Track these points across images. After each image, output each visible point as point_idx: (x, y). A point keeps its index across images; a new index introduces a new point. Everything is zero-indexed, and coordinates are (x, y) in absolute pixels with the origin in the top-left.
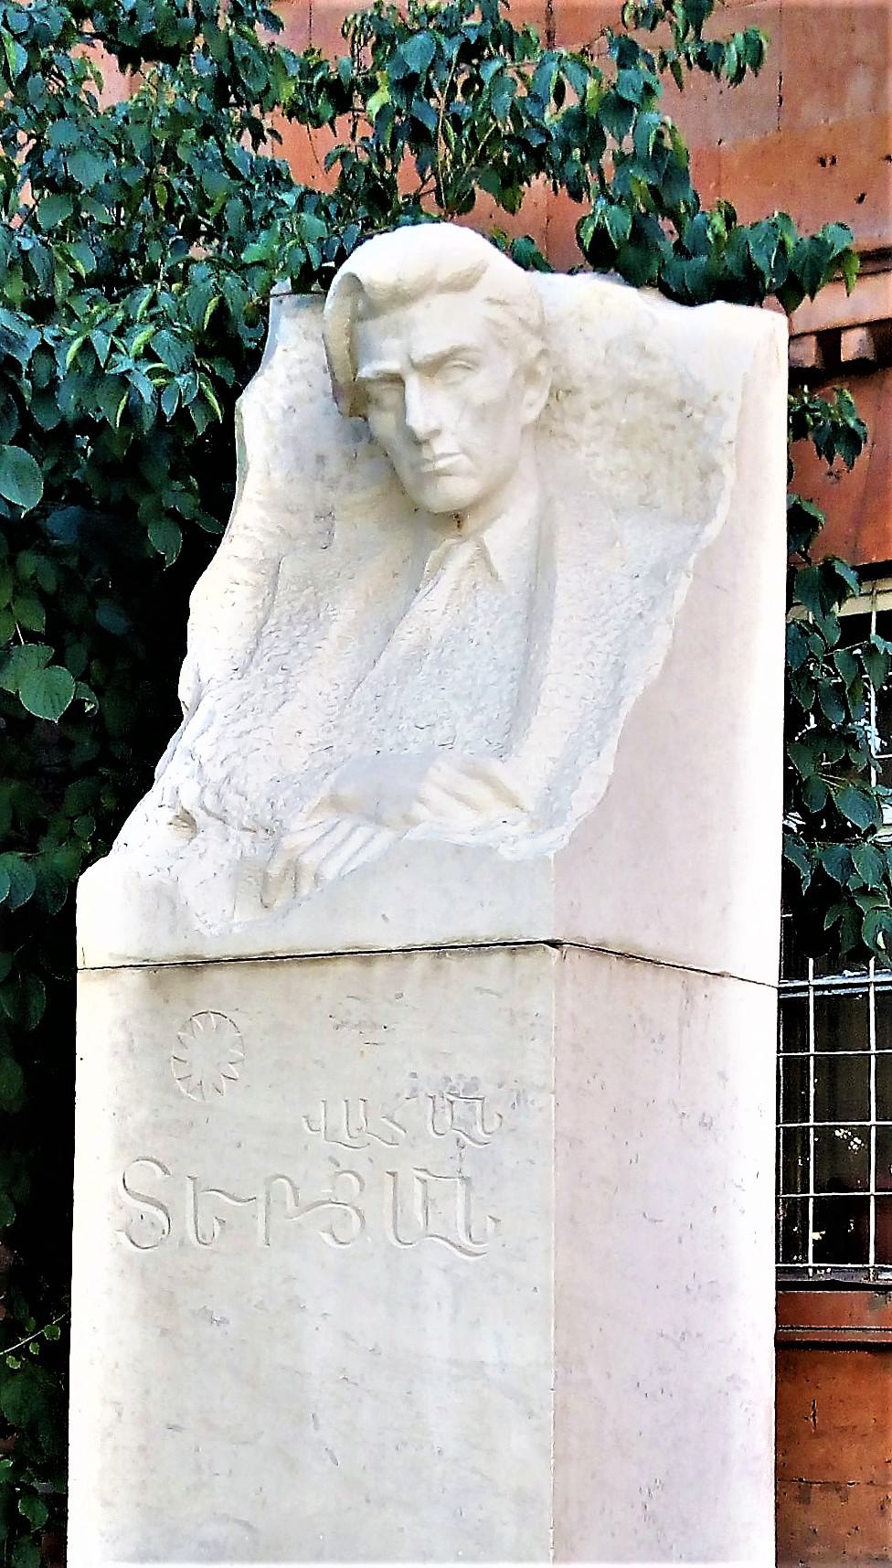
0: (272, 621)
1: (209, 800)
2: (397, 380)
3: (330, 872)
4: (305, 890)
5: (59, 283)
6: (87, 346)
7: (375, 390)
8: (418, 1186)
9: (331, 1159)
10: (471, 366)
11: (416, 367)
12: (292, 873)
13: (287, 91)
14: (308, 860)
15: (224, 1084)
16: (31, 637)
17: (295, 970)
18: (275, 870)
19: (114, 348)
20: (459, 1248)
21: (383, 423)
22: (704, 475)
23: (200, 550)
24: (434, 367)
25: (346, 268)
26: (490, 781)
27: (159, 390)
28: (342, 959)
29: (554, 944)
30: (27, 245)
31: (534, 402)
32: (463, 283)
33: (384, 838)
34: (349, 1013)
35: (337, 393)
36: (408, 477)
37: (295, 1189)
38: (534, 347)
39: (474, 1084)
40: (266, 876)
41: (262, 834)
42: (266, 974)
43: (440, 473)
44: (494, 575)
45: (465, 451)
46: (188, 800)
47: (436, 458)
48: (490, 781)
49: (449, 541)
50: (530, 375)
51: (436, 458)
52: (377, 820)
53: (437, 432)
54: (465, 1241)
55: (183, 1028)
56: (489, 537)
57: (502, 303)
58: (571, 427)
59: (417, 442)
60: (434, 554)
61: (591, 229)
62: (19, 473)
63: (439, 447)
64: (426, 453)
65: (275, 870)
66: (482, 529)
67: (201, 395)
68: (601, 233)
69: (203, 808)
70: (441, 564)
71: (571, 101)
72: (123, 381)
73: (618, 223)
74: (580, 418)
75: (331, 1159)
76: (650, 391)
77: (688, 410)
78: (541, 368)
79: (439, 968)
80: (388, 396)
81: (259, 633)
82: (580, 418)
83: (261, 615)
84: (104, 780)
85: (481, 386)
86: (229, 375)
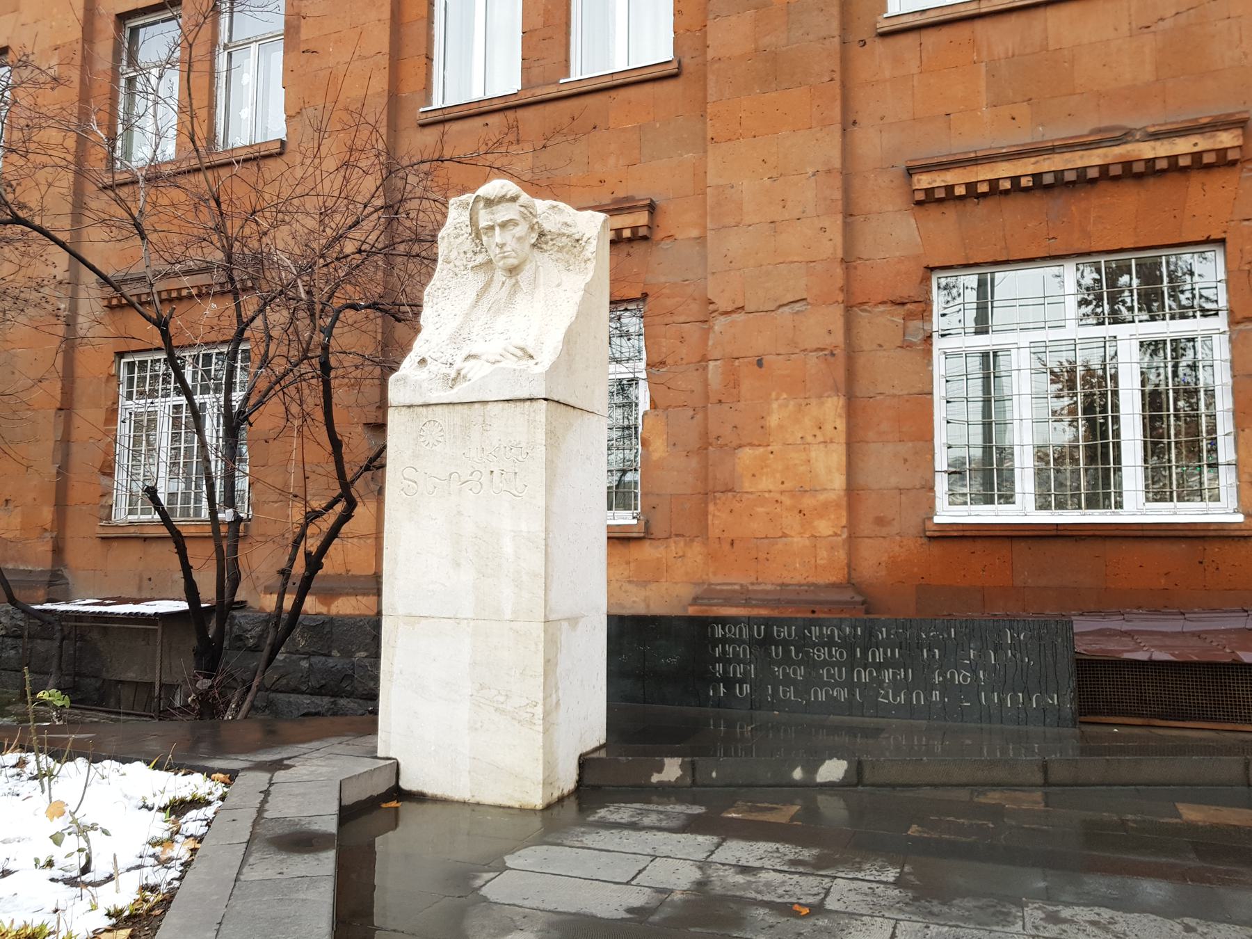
31: (535, 236)
32: (514, 199)
37: (459, 476)
58: (544, 246)
74: (546, 243)
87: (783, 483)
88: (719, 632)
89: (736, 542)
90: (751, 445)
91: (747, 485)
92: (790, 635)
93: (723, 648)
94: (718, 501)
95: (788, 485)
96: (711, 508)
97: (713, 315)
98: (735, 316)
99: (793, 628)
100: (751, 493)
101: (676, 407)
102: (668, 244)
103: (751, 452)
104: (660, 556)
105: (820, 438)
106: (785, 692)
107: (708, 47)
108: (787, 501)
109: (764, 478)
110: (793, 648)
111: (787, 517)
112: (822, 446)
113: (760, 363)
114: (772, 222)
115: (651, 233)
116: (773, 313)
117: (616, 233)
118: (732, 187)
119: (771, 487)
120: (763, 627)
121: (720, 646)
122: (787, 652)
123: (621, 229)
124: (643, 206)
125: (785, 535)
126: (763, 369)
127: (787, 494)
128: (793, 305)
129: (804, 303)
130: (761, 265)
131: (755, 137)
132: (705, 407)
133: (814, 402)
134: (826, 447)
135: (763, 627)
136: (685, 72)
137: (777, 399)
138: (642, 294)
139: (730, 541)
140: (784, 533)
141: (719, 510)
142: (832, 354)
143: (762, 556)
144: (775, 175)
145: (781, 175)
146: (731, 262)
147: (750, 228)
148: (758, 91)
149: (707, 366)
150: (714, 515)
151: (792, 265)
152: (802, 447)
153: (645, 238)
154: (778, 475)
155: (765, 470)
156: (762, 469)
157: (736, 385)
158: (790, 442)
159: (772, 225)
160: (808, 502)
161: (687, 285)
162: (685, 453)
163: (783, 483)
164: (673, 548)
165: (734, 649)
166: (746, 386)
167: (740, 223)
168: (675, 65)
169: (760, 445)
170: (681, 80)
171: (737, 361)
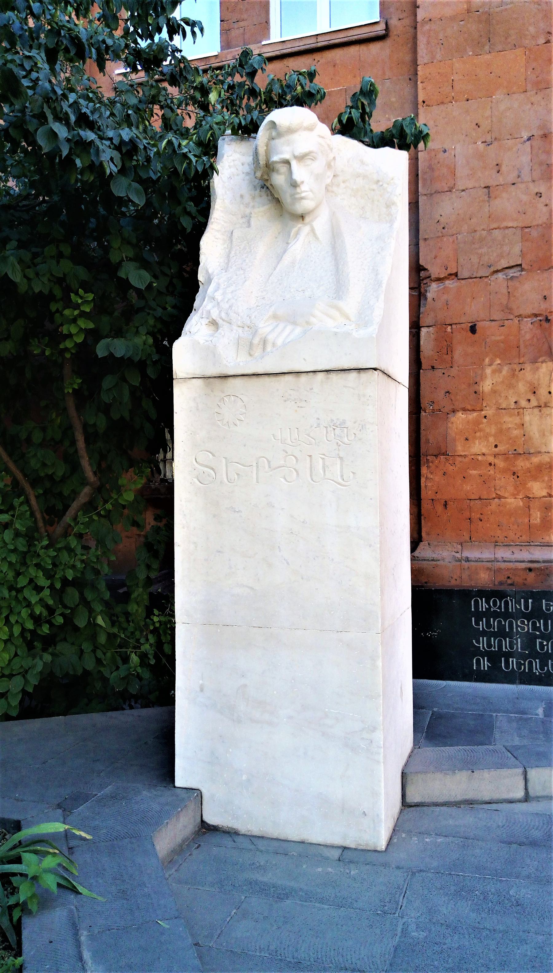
0: (233, 252)
1: (223, 315)
2: (287, 162)
3: (279, 342)
4: (269, 348)
8: (321, 461)
9: (284, 450)
10: (314, 159)
11: (295, 157)
12: (262, 343)
14: (271, 338)
15: (238, 422)
17: (267, 379)
20: (339, 484)
22: (388, 206)
24: (301, 158)
26: (338, 309)
28: (286, 376)
33: (298, 330)
34: (290, 395)
37: (269, 462)
39: (344, 422)
41: (246, 328)
43: (302, 198)
44: (317, 238)
45: (311, 191)
46: (215, 315)
47: (302, 192)
48: (338, 309)
49: (300, 225)
51: (302, 192)
52: (295, 323)
53: (303, 182)
54: (340, 481)
55: (220, 401)
56: (315, 224)
57: (323, 137)
60: (294, 230)
62: (137, 192)
63: (303, 188)
64: (298, 190)
65: (256, 341)
66: (312, 221)
69: (221, 318)
70: (297, 233)
74: (338, 186)
76: (365, 177)
77: (381, 183)
79: (328, 378)
80: (283, 169)
82: (338, 186)
83: (227, 250)
87: (496, 446)
88: (483, 605)
89: (450, 503)
90: (464, 410)
91: (460, 449)
93: (488, 622)
94: (431, 464)
95: (502, 448)
97: (425, 281)
100: (465, 456)
105: (534, 403)
107: (418, 7)
108: (500, 463)
109: (477, 442)
111: (500, 479)
112: (536, 411)
113: (473, 329)
114: (485, 187)
116: (486, 280)
118: (445, 151)
119: (484, 450)
128: (507, 271)
129: (519, 269)
130: (475, 231)
133: (528, 367)
134: (540, 411)
136: (394, 32)
137: (490, 365)
139: (443, 502)
140: (497, 494)
141: (432, 473)
142: (547, 320)
144: (489, 139)
145: (496, 139)
147: (463, 193)
148: (471, 53)
150: (427, 478)
151: (507, 231)
152: (516, 411)
154: (491, 439)
155: (478, 434)
157: (449, 350)
158: (504, 406)
160: (521, 464)
163: (496, 446)
166: (458, 353)
167: (452, 188)
168: (382, 26)
169: (474, 410)
170: (387, 43)
171: (449, 327)
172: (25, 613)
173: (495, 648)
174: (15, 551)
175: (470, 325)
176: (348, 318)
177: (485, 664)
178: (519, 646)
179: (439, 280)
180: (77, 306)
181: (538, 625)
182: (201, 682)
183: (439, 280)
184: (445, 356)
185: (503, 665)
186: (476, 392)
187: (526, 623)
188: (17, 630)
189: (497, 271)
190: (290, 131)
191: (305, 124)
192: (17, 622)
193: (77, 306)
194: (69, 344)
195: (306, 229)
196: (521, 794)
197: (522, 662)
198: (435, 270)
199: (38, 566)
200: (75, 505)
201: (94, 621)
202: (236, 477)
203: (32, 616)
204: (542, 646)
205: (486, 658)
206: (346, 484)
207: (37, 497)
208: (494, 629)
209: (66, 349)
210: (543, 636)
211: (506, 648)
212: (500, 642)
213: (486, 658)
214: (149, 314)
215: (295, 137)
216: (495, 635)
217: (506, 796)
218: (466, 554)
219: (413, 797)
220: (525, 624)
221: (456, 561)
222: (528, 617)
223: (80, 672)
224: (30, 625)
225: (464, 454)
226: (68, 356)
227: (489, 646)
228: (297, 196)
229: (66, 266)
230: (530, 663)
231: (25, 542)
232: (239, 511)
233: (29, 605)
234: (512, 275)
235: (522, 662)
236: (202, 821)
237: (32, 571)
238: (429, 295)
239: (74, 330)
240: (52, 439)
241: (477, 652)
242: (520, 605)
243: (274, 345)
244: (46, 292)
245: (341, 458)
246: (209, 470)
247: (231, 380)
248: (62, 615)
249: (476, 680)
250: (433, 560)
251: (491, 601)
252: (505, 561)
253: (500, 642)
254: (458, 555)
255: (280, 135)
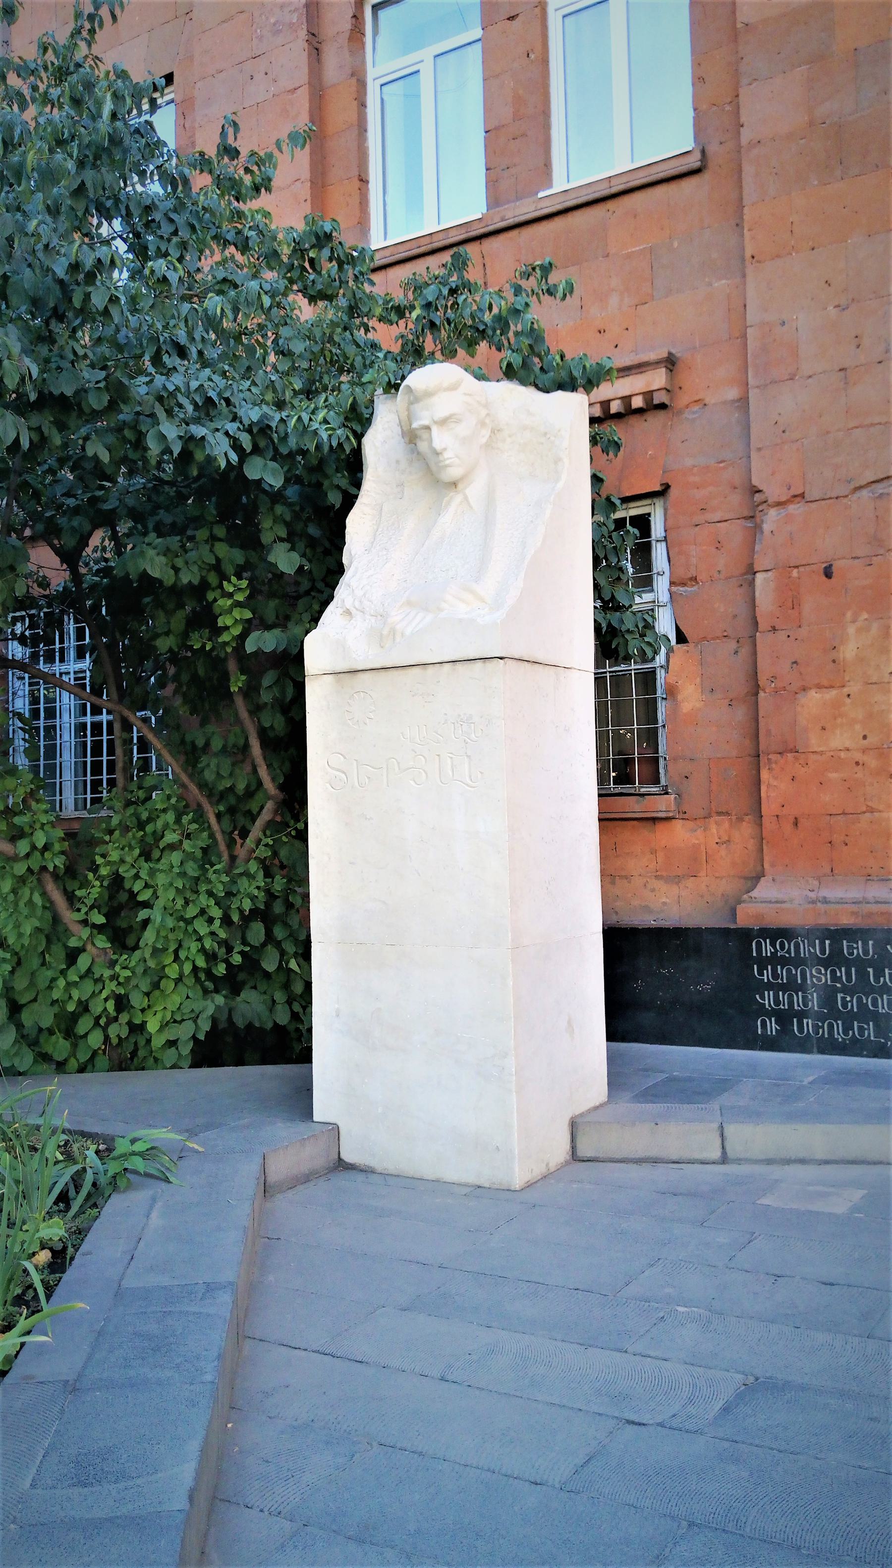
0: (380, 530)
1: (357, 604)
2: (428, 428)
3: (408, 632)
4: (398, 639)
5: (287, 393)
6: (300, 418)
7: (419, 433)
8: (449, 761)
9: (413, 750)
10: (458, 421)
11: (435, 422)
13: (378, 311)
15: (368, 721)
16: (282, 540)
18: (385, 632)
19: (311, 420)
20: (468, 785)
21: (423, 446)
22: (556, 463)
23: (349, 501)
24: (443, 422)
25: (405, 383)
27: (330, 436)
29: (501, 658)
30: (273, 378)
31: (486, 433)
32: (453, 388)
35: (404, 434)
36: (434, 468)
37: (398, 763)
38: (484, 412)
40: (381, 635)
41: (379, 617)
42: (383, 673)
45: (457, 457)
46: (348, 604)
47: (445, 460)
49: (451, 494)
50: (483, 424)
51: (445, 460)
53: (445, 449)
55: (350, 699)
56: (468, 491)
57: (470, 395)
59: (437, 454)
61: (505, 363)
62: (274, 473)
63: (446, 455)
64: (441, 458)
65: (385, 632)
67: (348, 437)
68: (509, 365)
70: (449, 503)
71: (495, 310)
72: (315, 432)
73: (517, 360)
75: (413, 750)
77: (548, 436)
78: (487, 421)
80: (424, 435)
81: (375, 535)
83: (375, 527)
84: (314, 597)
85: (463, 429)
86: (359, 429)
87: (865, 737)
88: (768, 949)
89: (803, 822)
90: (819, 687)
91: (814, 742)
92: (866, 952)
93: (774, 971)
94: (774, 766)
95: (873, 740)
96: (765, 775)
97: (760, 508)
98: (792, 508)
99: (871, 942)
100: (821, 753)
101: (713, 639)
102: (694, 413)
103: (818, 696)
104: (697, 842)
106: (861, 1029)
107: (742, 126)
109: (838, 732)
110: (870, 970)
113: (828, 573)
114: (840, 370)
115: (671, 399)
116: (845, 501)
117: (623, 402)
118: (783, 324)
119: (848, 744)
120: (827, 942)
121: (769, 967)
122: (863, 975)
123: (629, 397)
124: (657, 363)
125: (872, 810)
126: (833, 579)
127: (871, 752)
128: (874, 486)
130: (828, 432)
131: (813, 249)
132: (753, 637)
135: (827, 942)
136: (712, 164)
137: (854, 621)
138: (662, 485)
139: (792, 820)
140: (868, 806)
141: (776, 778)
143: (837, 838)
146: (784, 432)
147: (810, 380)
148: (816, 183)
149: (754, 579)
150: (769, 786)
151: (872, 429)
153: (663, 406)
154: (858, 727)
155: (839, 720)
156: (835, 718)
157: (796, 604)
158: (874, 679)
159: (842, 374)
161: (724, 468)
162: (727, 702)
163: (865, 737)
164: (714, 831)
165: (789, 971)
166: (808, 607)
167: (795, 375)
168: (697, 155)
169: (832, 687)
170: (706, 176)
171: (795, 571)
172: (194, 946)
173: (784, 1005)
174: (183, 874)
175: (825, 565)
176: (482, 600)
177: (773, 1027)
178: (815, 1003)
179: (779, 504)
180: (230, 595)
181: (838, 974)
182: (337, 1006)
183: (779, 504)
184: (790, 611)
185: (795, 1028)
186: (834, 661)
187: (823, 972)
188: (187, 968)
189: (861, 487)
190: (428, 394)
191: (445, 385)
192: (187, 958)
193: (230, 595)
194: (225, 637)
195: (458, 498)
196: (716, 1154)
197: (820, 1024)
198: (773, 491)
199: (210, 894)
200: (260, 823)
201: (287, 965)
202: (367, 780)
203: (203, 950)
204: (845, 1005)
205: (773, 1019)
206: (473, 785)
207: (219, 816)
208: (782, 979)
209: (226, 644)
210: (845, 990)
211: (799, 1006)
212: (790, 997)
213: (773, 1019)
214: (314, 597)
215: (435, 399)
216: (784, 988)
217: (697, 1156)
218: (825, 893)
219: (584, 1150)
220: (821, 973)
221: (809, 903)
222: (826, 963)
223: (269, 1025)
224: (201, 963)
225: (821, 749)
226: (229, 650)
227: (777, 1002)
228: (441, 464)
229: (222, 549)
230: (831, 1026)
231: (195, 866)
232: (371, 818)
233: (200, 939)
234: (881, 491)
235: (820, 1024)
236: (340, 1159)
237: (204, 900)
238: (767, 527)
239: (229, 622)
240: (234, 746)
241: (761, 1011)
242: (814, 948)
243: (403, 634)
244: (196, 582)
245: (468, 757)
246: (337, 773)
247: (360, 675)
248: (241, 953)
249: (762, 1048)
250: (777, 902)
251: (827, 952)
252: (877, 902)
253: (790, 997)
254: (813, 895)
255: (417, 400)
